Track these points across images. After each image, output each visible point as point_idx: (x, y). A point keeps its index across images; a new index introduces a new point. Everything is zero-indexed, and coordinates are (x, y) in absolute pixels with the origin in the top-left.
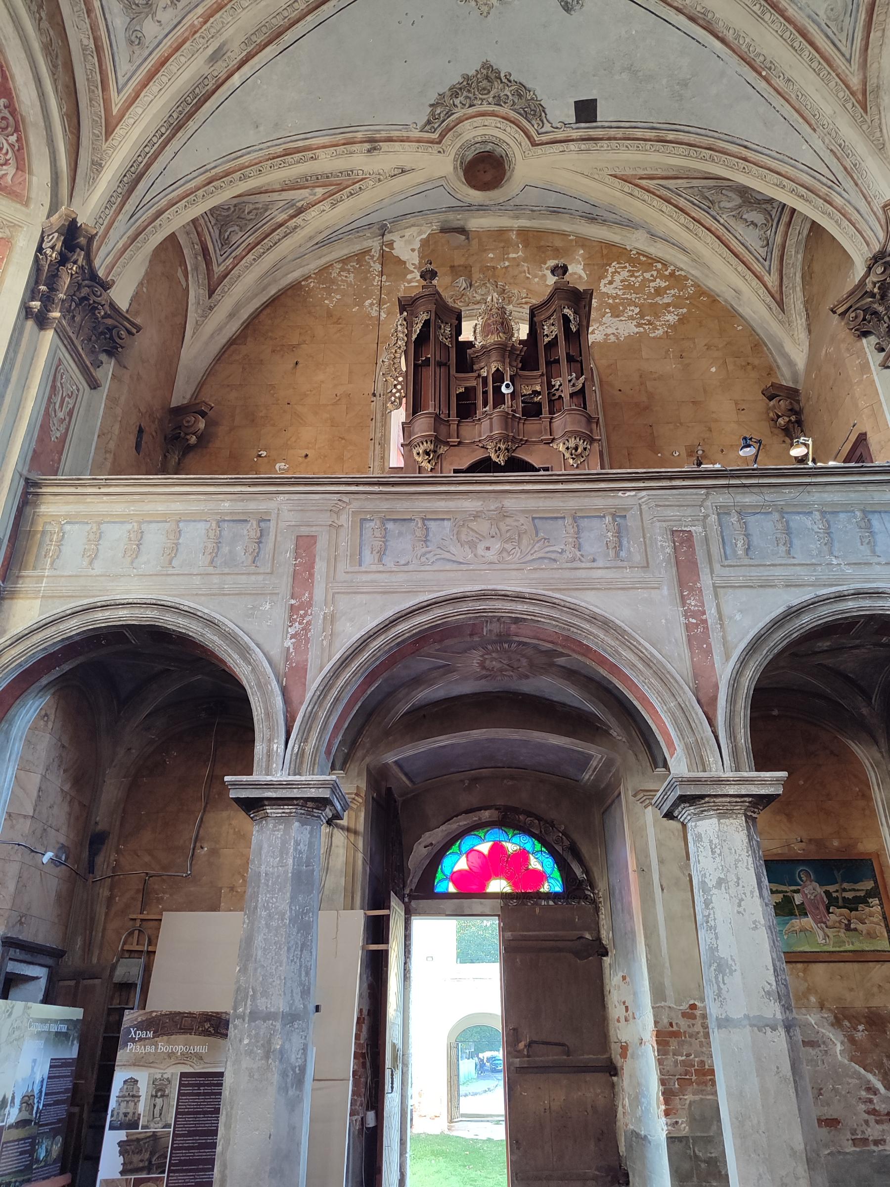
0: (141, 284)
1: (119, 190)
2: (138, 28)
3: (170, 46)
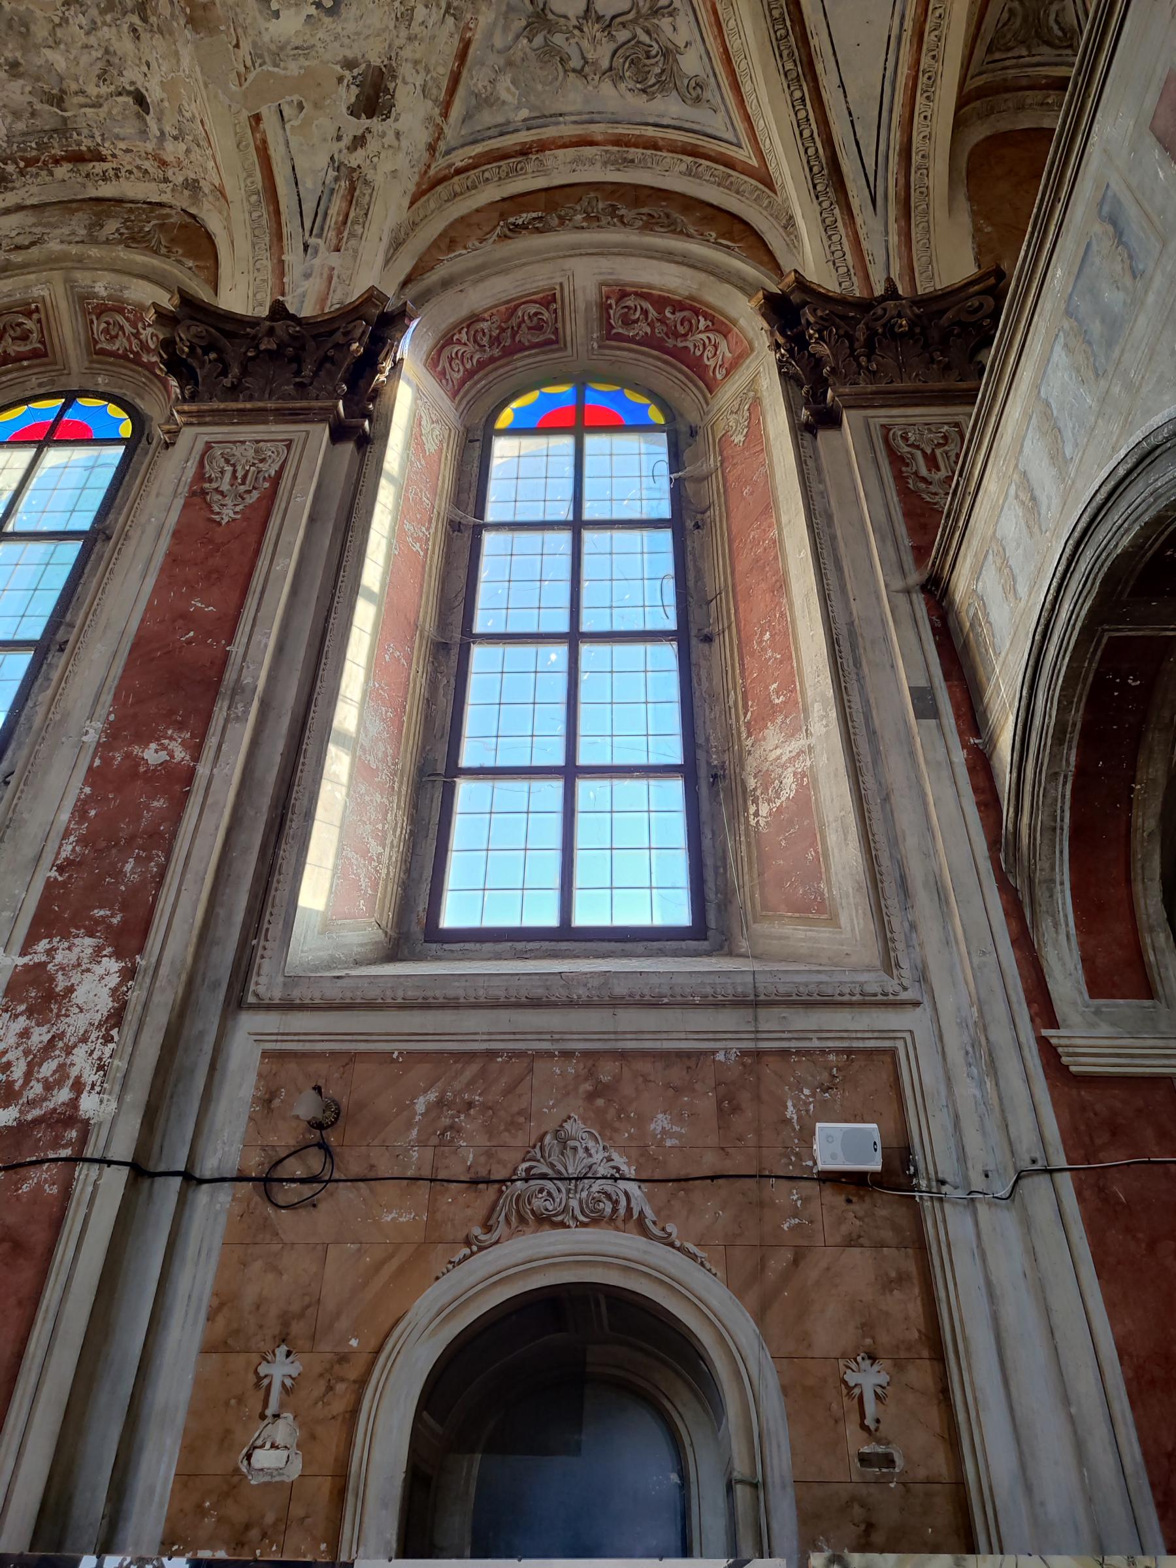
0: (977, 230)
1: (826, 204)
2: (686, 82)
3: (715, 38)
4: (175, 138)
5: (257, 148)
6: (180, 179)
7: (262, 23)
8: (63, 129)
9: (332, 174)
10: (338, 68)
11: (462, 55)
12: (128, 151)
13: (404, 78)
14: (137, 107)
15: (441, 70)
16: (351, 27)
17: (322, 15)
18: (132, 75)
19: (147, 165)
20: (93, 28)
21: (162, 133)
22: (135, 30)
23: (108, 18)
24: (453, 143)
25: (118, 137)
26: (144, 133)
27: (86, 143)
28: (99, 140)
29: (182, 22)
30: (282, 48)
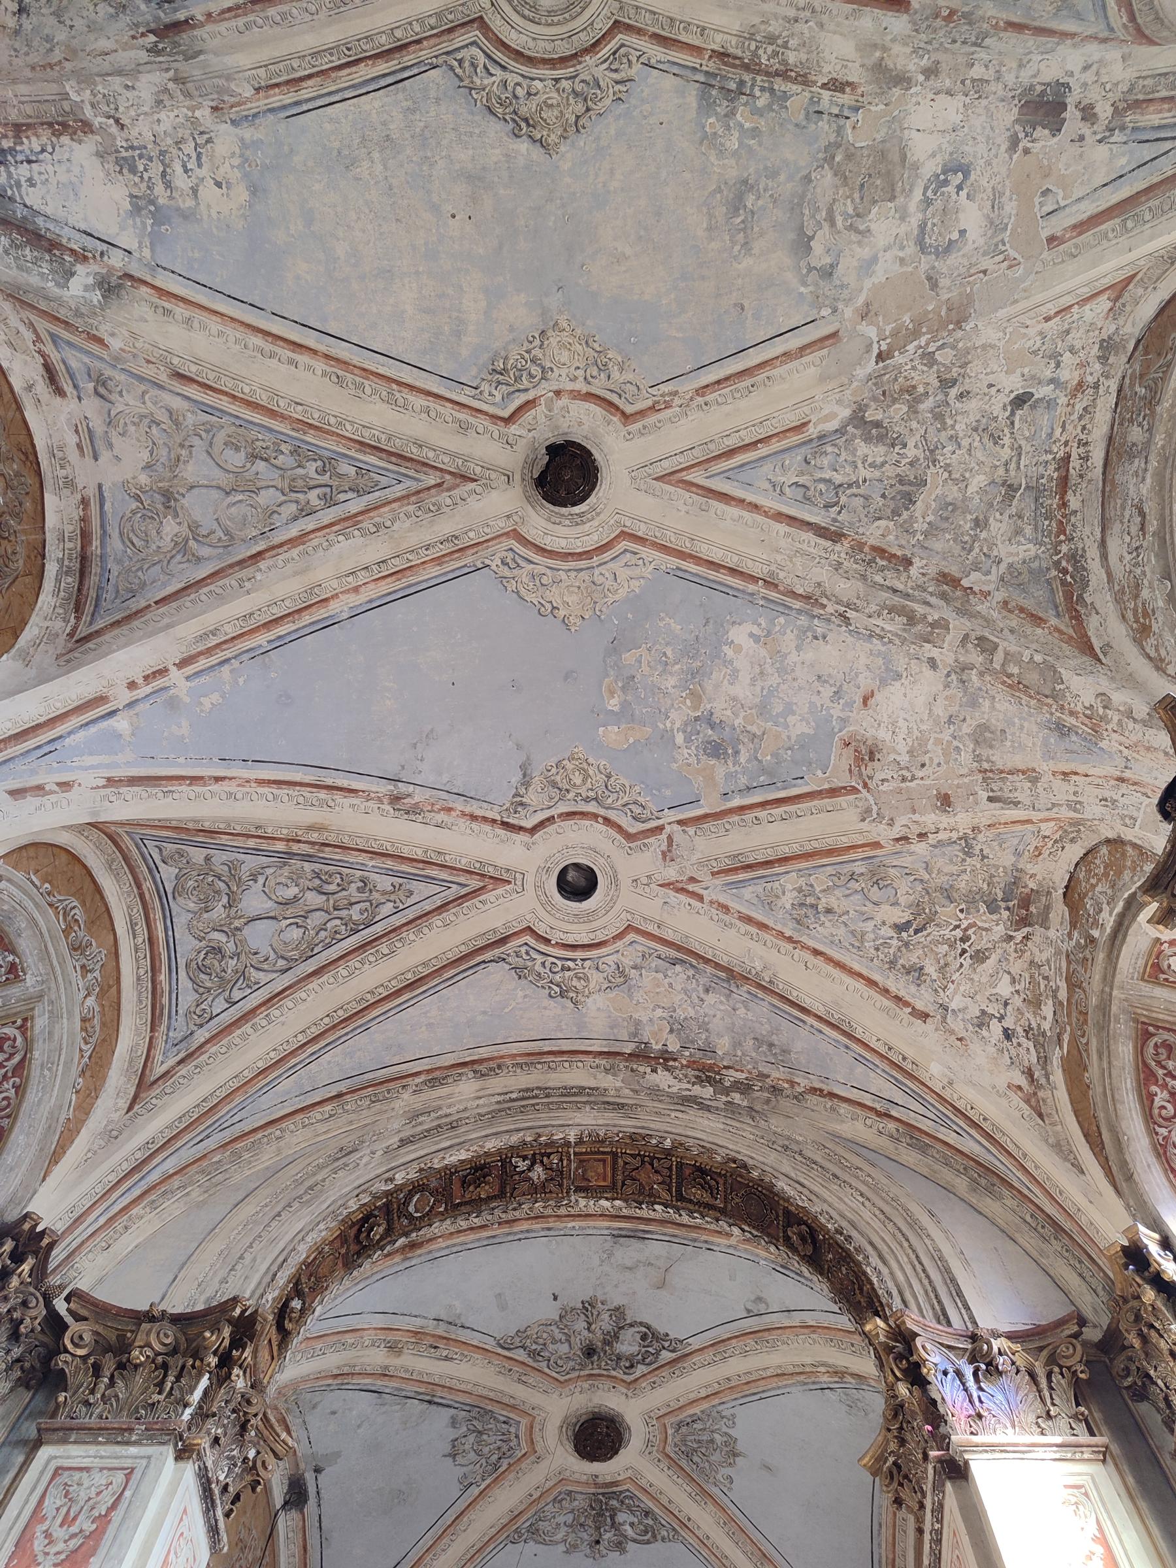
4: (1058, 365)
5: (1080, 234)
6: (1097, 366)
7: (970, 246)
8: (1036, 491)
9: (1118, 137)
10: (1015, 157)
11: (1018, 27)
12: (1063, 427)
13: (1035, 76)
14: (1026, 407)
15: (1031, 43)
16: (982, 149)
17: (968, 183)
18: (998, 406)
19: (1079, 407)
20: (954, 438)
21: (1052, 381)
22: (961, 395)
23: (949, 422)
24: (1103, 26)
25: (1050, 435)
26: (1050, 404)
27: (1051, 471)
28: (1050, 457)
29: (959, 334)
30: (992, 223)
